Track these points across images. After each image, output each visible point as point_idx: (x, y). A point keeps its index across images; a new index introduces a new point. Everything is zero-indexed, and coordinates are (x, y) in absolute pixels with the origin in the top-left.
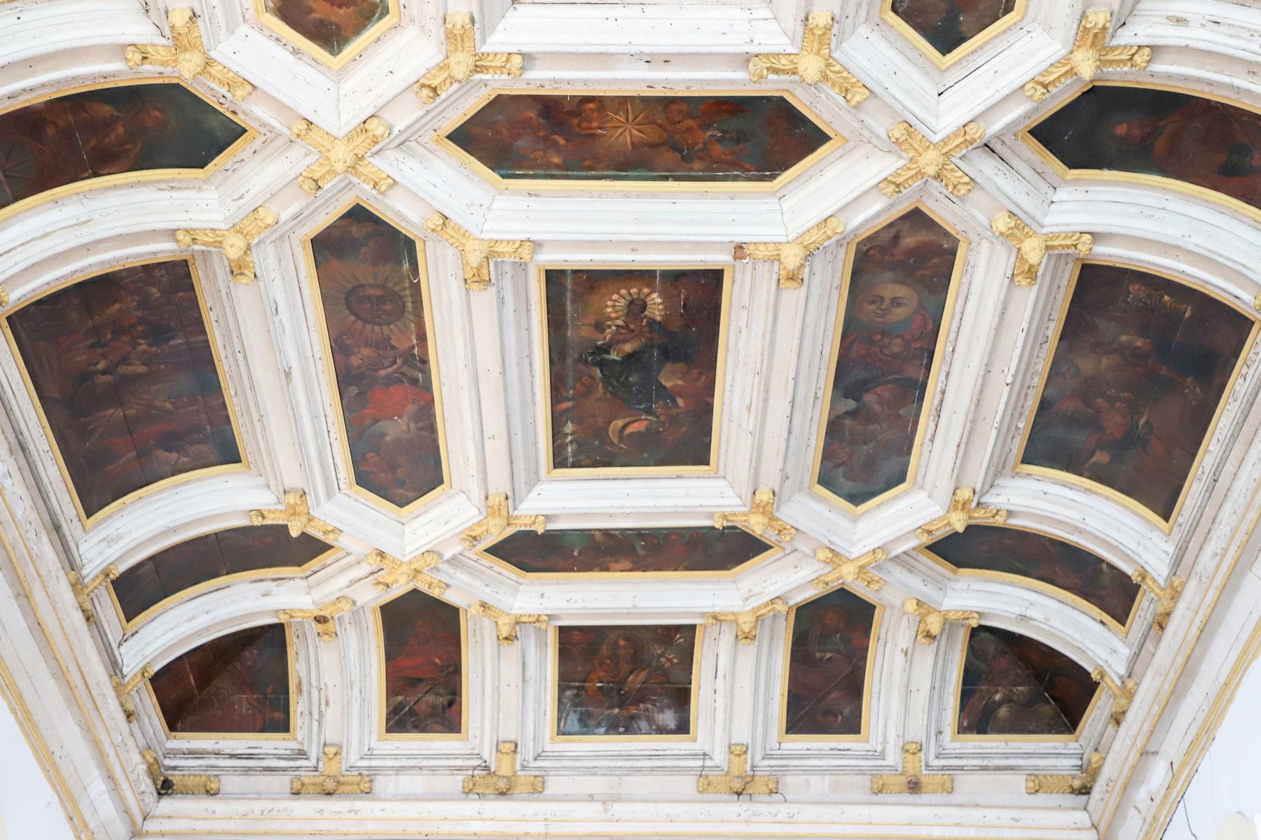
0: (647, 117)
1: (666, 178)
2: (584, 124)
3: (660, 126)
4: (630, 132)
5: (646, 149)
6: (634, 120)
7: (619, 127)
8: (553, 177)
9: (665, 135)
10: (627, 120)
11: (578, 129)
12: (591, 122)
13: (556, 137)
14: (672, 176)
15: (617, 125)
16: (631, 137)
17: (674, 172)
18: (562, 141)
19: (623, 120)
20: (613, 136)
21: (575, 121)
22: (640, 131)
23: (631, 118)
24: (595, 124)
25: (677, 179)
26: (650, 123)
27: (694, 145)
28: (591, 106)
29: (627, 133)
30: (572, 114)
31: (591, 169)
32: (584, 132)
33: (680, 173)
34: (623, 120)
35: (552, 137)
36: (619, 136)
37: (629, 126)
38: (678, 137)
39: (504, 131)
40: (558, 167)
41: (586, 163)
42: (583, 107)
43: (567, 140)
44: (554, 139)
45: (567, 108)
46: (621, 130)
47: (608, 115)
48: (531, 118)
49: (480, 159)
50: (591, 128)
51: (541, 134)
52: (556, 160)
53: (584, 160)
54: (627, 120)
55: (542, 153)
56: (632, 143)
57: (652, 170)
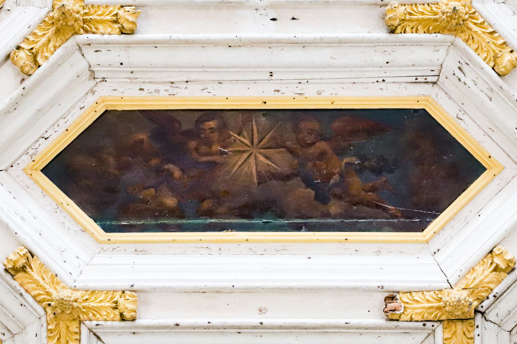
0: (273, 138)
1: (298, 228)
2: (204, 149)
3: (291, 151)
4: (256, 157)
5: (274, 182)
6: (260, 142)
7: (244, 152)
8: (164, 228)
9: (296, 161)
10: (252, 143)
11: (195, 155)
12: (209, 143)
13: (170, 166)
14: (305, 224)
15: (241, 149)
16: (256, 164)
17: (308, 218)
18: (177, 173)
19: (247, 142)
20: (234, 165)
21: (193, 144)
22: (267, 158)
23: (256, 141)
24: (217, 148)
25: (311, 228)
26: (278, 146)
27: (330, 175)
28: (212, 124)
29: (252, 160)
30: (190, 134)
31: (210, 214)
32: (204, 159)
33: (314, 220)
34: (247, 142)
35: (166, 167)
36: (242, 164)
37: (255, 151)
38: (310, 164)
39: (111, 160)
40: (173, 213)
41: (206, 205)
42: (202, 126)
43: (183, 171)
44: (168, 170)
45: (186, 126)
46: (245, 155)
47: (230, 136)
48: (142, 141)
49: (79, 204)
50: (211, 154)
51: (154, 162)
52: (171, 201)
53: (203, 201)
54: (252, 143)
55: (153, 190)
56: (258, 172)
57: (281, 217)
